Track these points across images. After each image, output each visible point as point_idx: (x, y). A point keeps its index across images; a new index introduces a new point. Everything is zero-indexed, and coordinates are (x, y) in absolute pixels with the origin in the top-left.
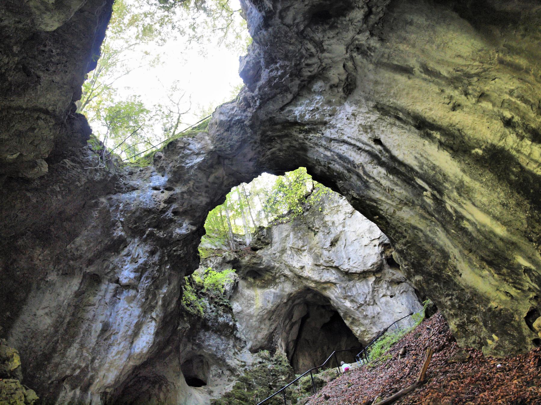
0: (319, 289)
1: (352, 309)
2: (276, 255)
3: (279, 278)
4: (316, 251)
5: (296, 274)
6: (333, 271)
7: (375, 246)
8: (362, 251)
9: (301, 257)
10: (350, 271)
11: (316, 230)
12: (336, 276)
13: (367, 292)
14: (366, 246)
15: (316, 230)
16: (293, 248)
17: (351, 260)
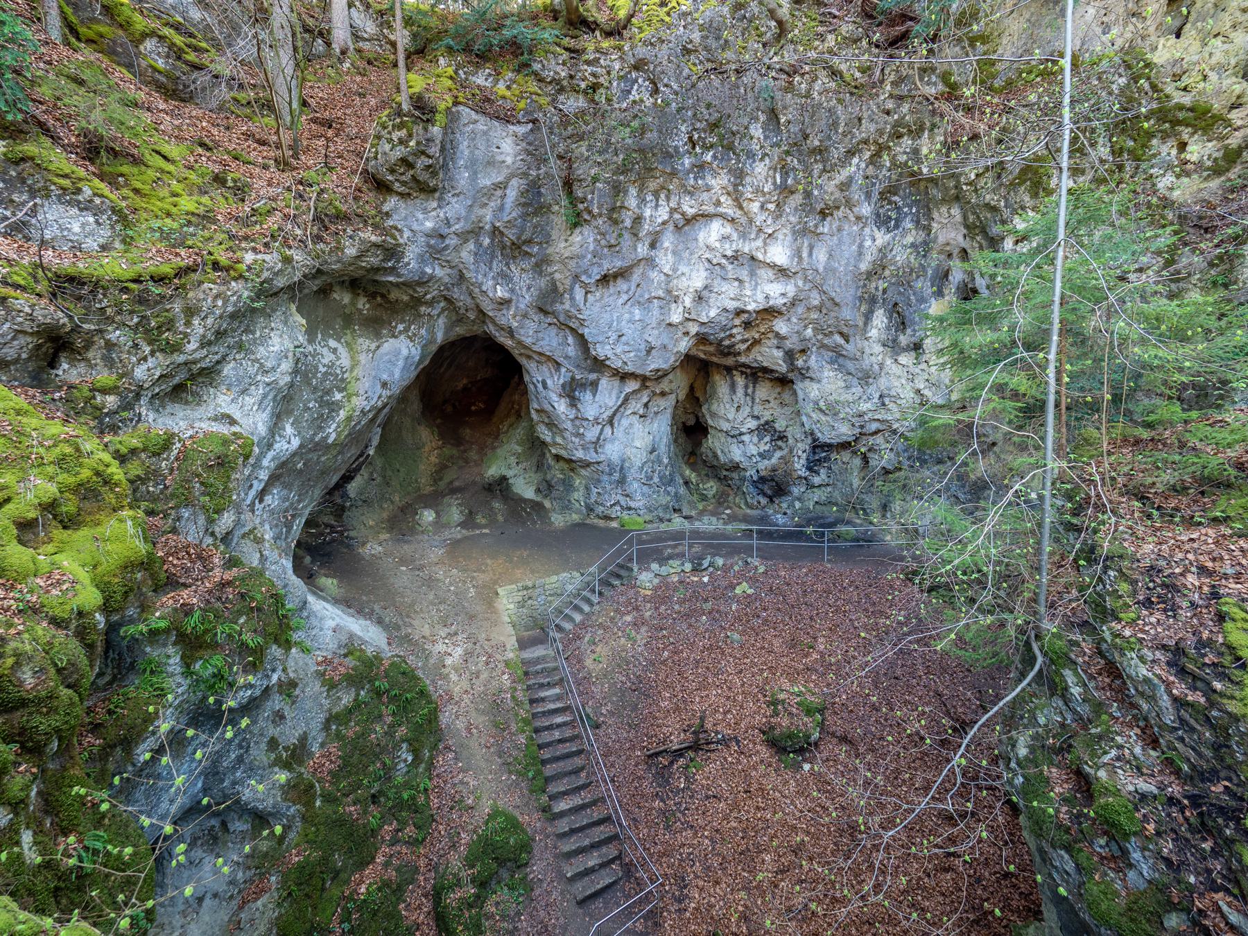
0: (515, 353)
1: (563, 417)
2: (447, 242)
3: (430, 304)
4: (557, 276)
5: (478, 306)
6: (570, 340)
7: (686, 334)
9: (513, 267)
10: (608, 363)
11: (586, 217)
12: (572, 350)
13: (611, 404)
14: (670, 324)
15: (586, 217)
16: (502, 233)
17: (623, 338)
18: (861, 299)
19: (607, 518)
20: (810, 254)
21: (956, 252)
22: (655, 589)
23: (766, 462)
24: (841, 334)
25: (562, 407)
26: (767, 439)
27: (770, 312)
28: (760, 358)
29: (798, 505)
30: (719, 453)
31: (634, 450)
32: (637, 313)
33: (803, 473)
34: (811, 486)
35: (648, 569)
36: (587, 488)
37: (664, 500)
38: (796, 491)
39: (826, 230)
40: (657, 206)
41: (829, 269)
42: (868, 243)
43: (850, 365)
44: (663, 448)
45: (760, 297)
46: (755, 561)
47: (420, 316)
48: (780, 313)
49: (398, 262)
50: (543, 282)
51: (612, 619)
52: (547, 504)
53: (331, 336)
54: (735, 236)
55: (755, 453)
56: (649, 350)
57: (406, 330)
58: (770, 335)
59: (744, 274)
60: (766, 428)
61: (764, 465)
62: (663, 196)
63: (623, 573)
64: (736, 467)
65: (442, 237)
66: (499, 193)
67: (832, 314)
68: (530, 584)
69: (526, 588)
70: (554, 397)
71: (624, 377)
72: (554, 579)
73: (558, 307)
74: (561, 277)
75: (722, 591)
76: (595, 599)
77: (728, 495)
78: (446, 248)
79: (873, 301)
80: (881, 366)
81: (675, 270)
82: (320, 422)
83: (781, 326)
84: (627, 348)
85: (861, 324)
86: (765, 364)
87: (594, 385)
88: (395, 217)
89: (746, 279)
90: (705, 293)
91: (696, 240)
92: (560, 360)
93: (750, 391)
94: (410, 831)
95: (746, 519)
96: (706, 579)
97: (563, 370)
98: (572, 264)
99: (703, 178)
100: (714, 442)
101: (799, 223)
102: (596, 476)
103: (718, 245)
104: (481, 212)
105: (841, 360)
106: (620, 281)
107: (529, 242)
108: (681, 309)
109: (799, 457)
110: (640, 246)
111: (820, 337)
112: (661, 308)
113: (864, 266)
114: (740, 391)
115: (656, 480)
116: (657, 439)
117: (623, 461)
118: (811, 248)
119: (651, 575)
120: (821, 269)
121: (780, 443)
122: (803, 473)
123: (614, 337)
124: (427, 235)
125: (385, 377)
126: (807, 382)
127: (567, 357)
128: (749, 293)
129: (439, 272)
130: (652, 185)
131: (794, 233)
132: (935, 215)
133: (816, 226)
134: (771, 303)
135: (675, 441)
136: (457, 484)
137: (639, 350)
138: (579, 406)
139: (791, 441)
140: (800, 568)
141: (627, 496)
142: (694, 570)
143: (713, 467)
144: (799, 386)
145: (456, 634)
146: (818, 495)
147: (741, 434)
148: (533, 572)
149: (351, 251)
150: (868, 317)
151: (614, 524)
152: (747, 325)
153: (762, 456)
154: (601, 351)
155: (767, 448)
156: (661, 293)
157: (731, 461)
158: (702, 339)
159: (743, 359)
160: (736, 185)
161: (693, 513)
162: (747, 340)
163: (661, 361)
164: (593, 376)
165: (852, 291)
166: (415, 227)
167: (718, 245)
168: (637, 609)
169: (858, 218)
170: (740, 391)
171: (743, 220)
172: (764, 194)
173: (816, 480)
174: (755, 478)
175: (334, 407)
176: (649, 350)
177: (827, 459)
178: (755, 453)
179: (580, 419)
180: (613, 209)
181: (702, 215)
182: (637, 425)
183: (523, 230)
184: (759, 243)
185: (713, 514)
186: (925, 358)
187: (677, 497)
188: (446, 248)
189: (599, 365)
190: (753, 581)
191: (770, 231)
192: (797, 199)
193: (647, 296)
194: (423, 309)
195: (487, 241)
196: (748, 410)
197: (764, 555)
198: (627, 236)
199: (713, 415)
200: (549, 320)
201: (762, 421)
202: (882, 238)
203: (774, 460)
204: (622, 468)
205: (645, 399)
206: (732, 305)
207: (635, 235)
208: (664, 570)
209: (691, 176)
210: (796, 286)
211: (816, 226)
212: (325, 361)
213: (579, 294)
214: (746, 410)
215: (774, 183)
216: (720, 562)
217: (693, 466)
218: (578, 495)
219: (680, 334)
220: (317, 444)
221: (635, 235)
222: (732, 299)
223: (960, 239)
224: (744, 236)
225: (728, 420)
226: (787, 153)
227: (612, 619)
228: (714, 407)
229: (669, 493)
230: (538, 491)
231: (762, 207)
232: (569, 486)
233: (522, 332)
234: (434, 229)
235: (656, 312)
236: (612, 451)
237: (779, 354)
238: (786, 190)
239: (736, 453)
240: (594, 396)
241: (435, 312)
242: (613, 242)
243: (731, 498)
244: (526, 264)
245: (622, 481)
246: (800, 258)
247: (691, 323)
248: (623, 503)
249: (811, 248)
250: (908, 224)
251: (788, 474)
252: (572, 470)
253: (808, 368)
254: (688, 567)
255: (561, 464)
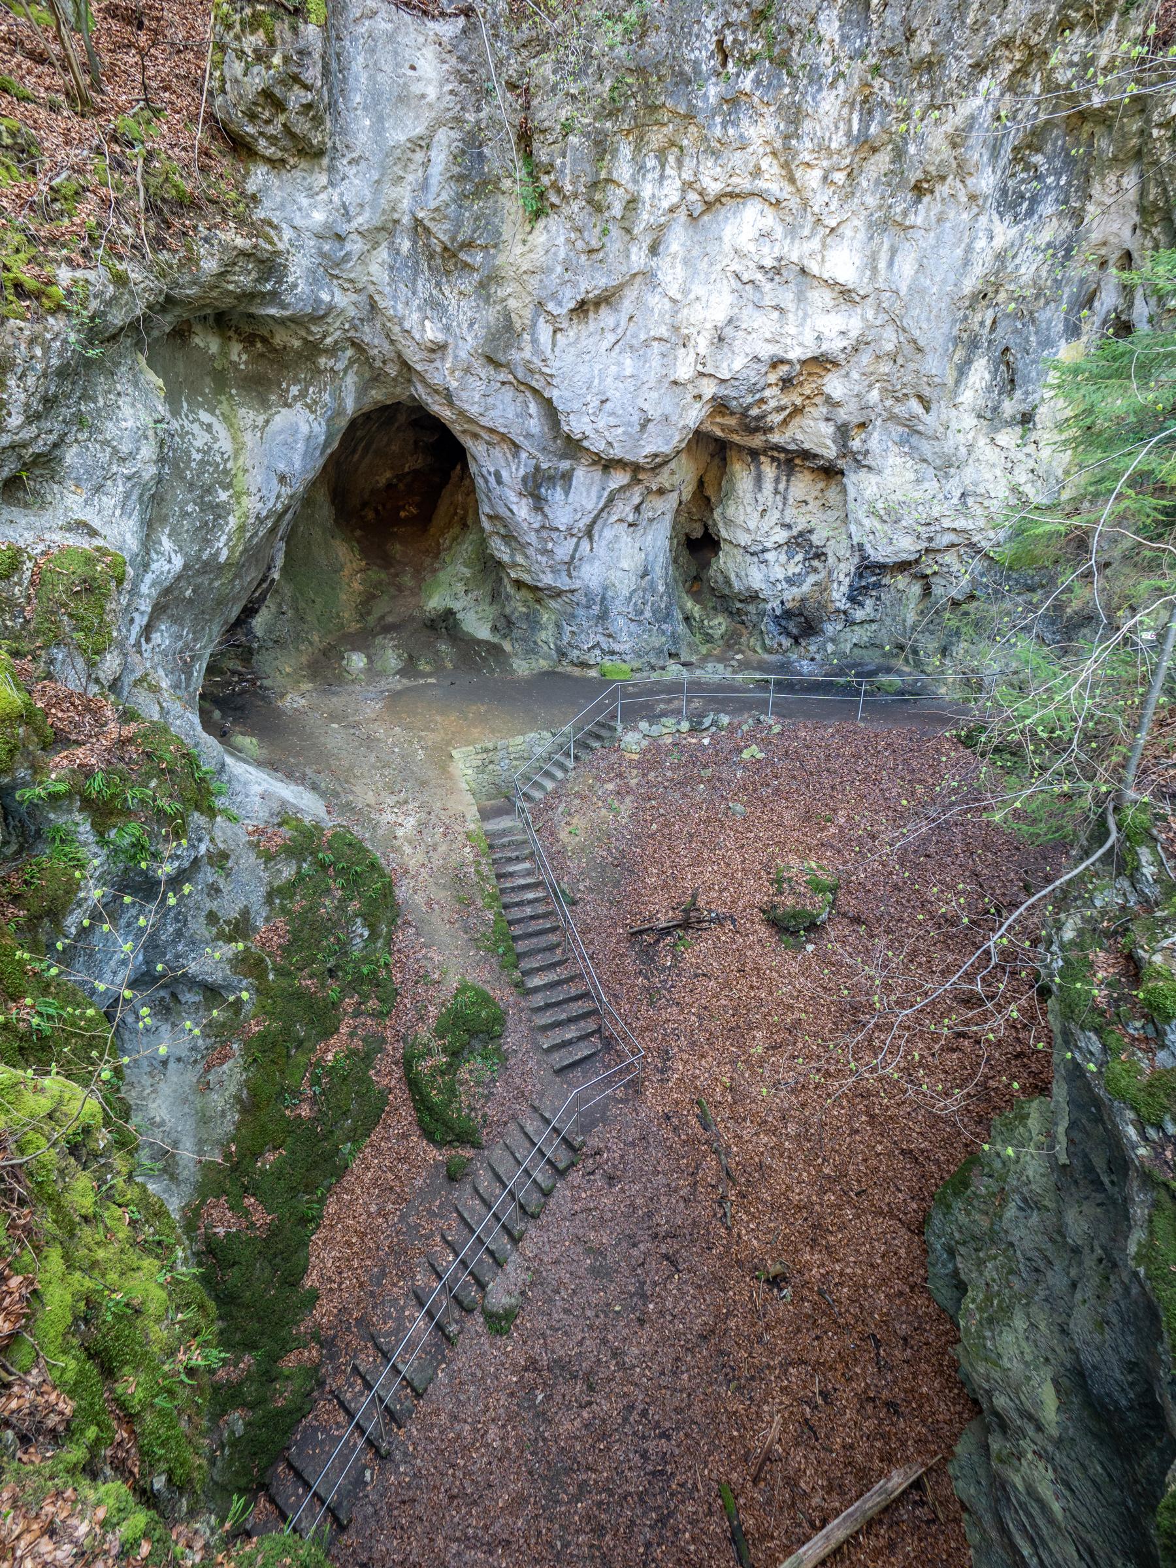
0: (456, 429)
1: (525, 525)
2: (348, 246)
3: (332, 352)
4: (512, 303)
5: (400, 355)
6: (533, 408)
8: (654, 395)
9: (447, 290)
10: (585, 444)
11: (554, 199)
12: (535, 424)
13: (589, 507)
14: (675, 383)
15: (554, 199)
16: (427, 230)
17: (608, 405)
18: (957, 340)
19: (584, 665)
20: (891, 264)
21: (1114, 258)
22: (644, 752)
23: (795, 590)
24: (920, 397)
25: (522, 510)
26: (800, 557)
27: (822, 363)
28: (800, 437)
29: (830, 647)
30: (733, 577)
31: (620, 573)
32: (629, 365)
33: (843, 604)
34: (850, 623)
35: (635, 729)
36: (558, 626)
37: (658, 641)
38: (830, 629)
39: (919, 221)
40: (662, 177)
41: (917, 290)
42: (981, 243)
43: (926, 448)
44: (658, 571)
45: (809, 338)
46: (770, 720)
47: (320, 372)
48: (836, 364)
49: (280, 282)
50: (491, 315)
51: (591, 787)
52: (507, 646)
53: (201, 406)
54: (779, 232)
55: (781, 577)
56: (645, 424)
57: (303, 394)
58: (817, 400)
59: (787, 297)
60: (800, 542)
61: (792, 594)
62: (671, 159)
63: (604, 733)
64: (754, 597)
65: (340, 238)
66: (419, 156)
67: (912, 366)
68: (490, 746)
69: (487, 751)
70: (512, 497)
71: (608, 465)
72: (519, 739)
73: (515, 356)
74: (519, 306)
75: (725, 755)
76: (570, 763)
77: (741, 635)
78: (347, 258)
79: (973, 344)
80: (970, 447)
81: (685, 292)
82: (205, 532)
83: (835, 386)
84: (613, 421)
85: (950, 382)
86: (806, 446)
87: (567, 477)
88: (267, 203)
89: (791, 306)
90: (729, 332)
91: (720, 238)
92: (519, 440)
93: (782, 487)
94: (373, 1004)
95: (762, 667)
96: (706, 741)
97: (524, 455)
98: (533, 282)
99: (736, 124)
100: (727, 562)
101: (880, 207)
102: (569, 610)
103: (752, 247)
104: (394, 192)
105: (914, 440)
106: (604, 310)
107: (468, 245)
108: (692, 358)
109: (840, 583)
110: (634, 250)
111: (889, 403)
112: (664, 355)
113: (969, 285)
114: (768, 486)
115: (648, 614)
116: (650, 558)
117: (605, 588)
118: (893, 251)
119: (638, 736)
120: (903, 291)
121: (816, 563)
122: (843, 604)
123: (595, 403)
124: (318, 236)
125: (282, 467)
126: (863, 473)
127: (528, 436)
128: (792, 330)
129: (342, 300)
130: (657, 138)
131: (870, 225)
132: (1096, 190)
133: (905, 213)
134: (824, 348)
135: (675, 561)
136: (390, 619)
137: (630, 424)
138: (546, 509)
139: (831, 560)
140: (826, 728)
141: (610, 636)
142: (693, 730)
143: (723, 597)
144: (851, 480)
145: (406, 802)
146: (860, 635)
147: (764, 551)
148: (493, 731)
149: (210, 266)
150: (962, 370)
151: (593, 673)
152: (787, 383)
153: (791, 581)
154: (576, 425)
155: (797, 570)
156: (663, 331)
157: (748, 589)
158: (720, 406)
159: (775, 438)
160: (787, 137)
161: (694, 659)
162: (783, 408)
163: (660, 441)
164: (565, 465)
165: (945, 328)
166: (298, 222)
167: (752, 247)
168: (620, 775)
169: (973, 198)
170: (768, 486)
171: (794, 203)
172: (830, 155)
173: (859, 615)
174: (778, 612)
175: (220, 512)
176: (645, 424)
177: (877, 585)
178: (781, 577)
179: (547, 528)
180: (594, 185)
181: (731, 195)
182: (626, 539)
183: (459, 225)
184: (815, 244)
185: (720, 660)
186: (1034, 436)
187: (675, 638)
188: (347, 258)
189: (573, 447)
190: (765, 744)
191: (833, 224)
192: (882, 161)
193: (643, 337)
194: (323, 361)
195: (406, 245)
196: (777, 514)
197: (782, 712)
198: (615, 232)
199: (729, 522)
200: (502, 376)
201: (795, 532)
202: (1004, 232)
203: (805, 588)
204: (603, 598)
205: (636, 500)
206: (767, 351)
207: (628, 231)
208: (655, 730)
209: (718, 119)
210: (864, 319)
211: (905, 213)
212: (199, 443)
213: (544, 332)
214: (774, 516)
215: (848, 133)
216: (725, 720)
217: (696, 596)
218: (546, 635)
219: (689, 397)
220: (206, 564)
221: (628, 231)
222: (767, 341)
223: (1127, 232)
224: (792, 230)
225: (748, 530)
226: (876, 70)
227: (591, 787)
228: (731, 511)
229: (663, 633)
230: (495, 629)
231: (825, 178)
232: (534, 623)
233: (464, 395)
234: (327, 226)
235: (656, 363)
236: (591, 575)
237: (828, 429)
238: (865, 146)
239: (756, 578)
240: (567, 494)
241: (340, 366)
242: (594, 244)
243: (744, 640)
244: (467, 284)
245: (603, 616)
246: (875, 270)
247: (705, 381)
248: (605, 646)
249: (893, 251)
250: (1047, 208)
251: (822, 606)
252: (538, 601)
253: (867, 451)
254: (685, 726)
255: (524, 594)
